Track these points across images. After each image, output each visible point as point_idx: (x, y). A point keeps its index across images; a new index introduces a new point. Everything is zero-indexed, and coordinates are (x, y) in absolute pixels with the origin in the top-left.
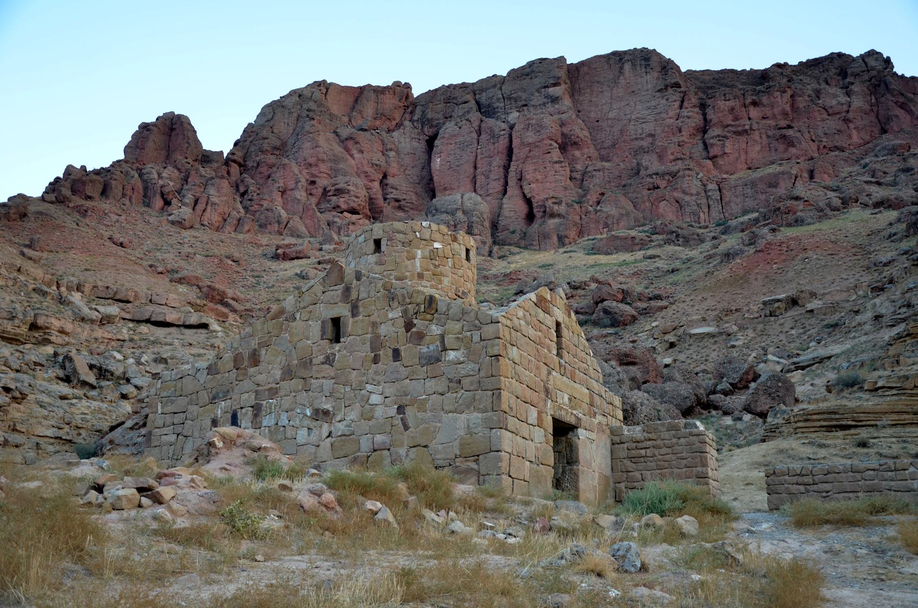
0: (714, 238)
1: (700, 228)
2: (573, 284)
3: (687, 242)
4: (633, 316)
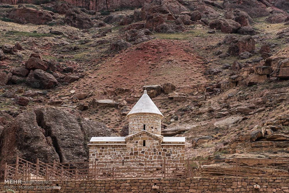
0: (101, 25)
1: (90, 13)
2: (5, 49)
3: (80, 25)
4: (55, 83)
